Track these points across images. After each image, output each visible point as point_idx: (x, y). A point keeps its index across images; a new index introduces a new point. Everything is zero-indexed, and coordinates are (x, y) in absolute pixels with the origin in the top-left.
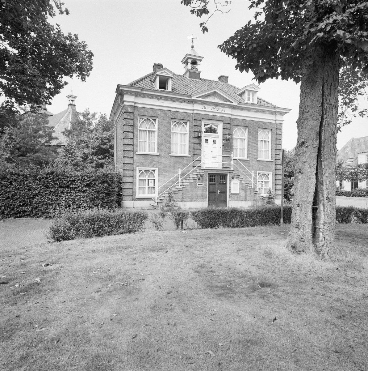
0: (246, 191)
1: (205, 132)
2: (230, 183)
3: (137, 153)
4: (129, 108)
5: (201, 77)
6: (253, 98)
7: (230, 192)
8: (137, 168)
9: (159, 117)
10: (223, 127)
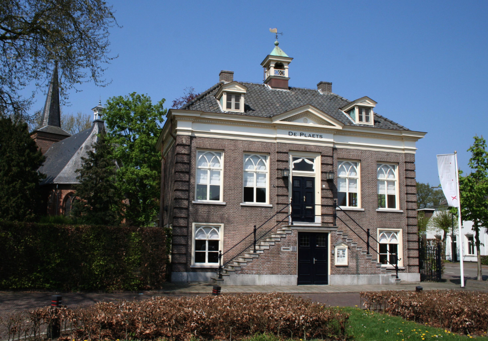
0: (357, 260)
1: (294, 169)
2: (333, 247)
3: (193, 202)
4: (184, 140)
6: (366, 117)
7: (332, 260)
8: (193, 224)
9: (226, 149)
10: (322, 161)
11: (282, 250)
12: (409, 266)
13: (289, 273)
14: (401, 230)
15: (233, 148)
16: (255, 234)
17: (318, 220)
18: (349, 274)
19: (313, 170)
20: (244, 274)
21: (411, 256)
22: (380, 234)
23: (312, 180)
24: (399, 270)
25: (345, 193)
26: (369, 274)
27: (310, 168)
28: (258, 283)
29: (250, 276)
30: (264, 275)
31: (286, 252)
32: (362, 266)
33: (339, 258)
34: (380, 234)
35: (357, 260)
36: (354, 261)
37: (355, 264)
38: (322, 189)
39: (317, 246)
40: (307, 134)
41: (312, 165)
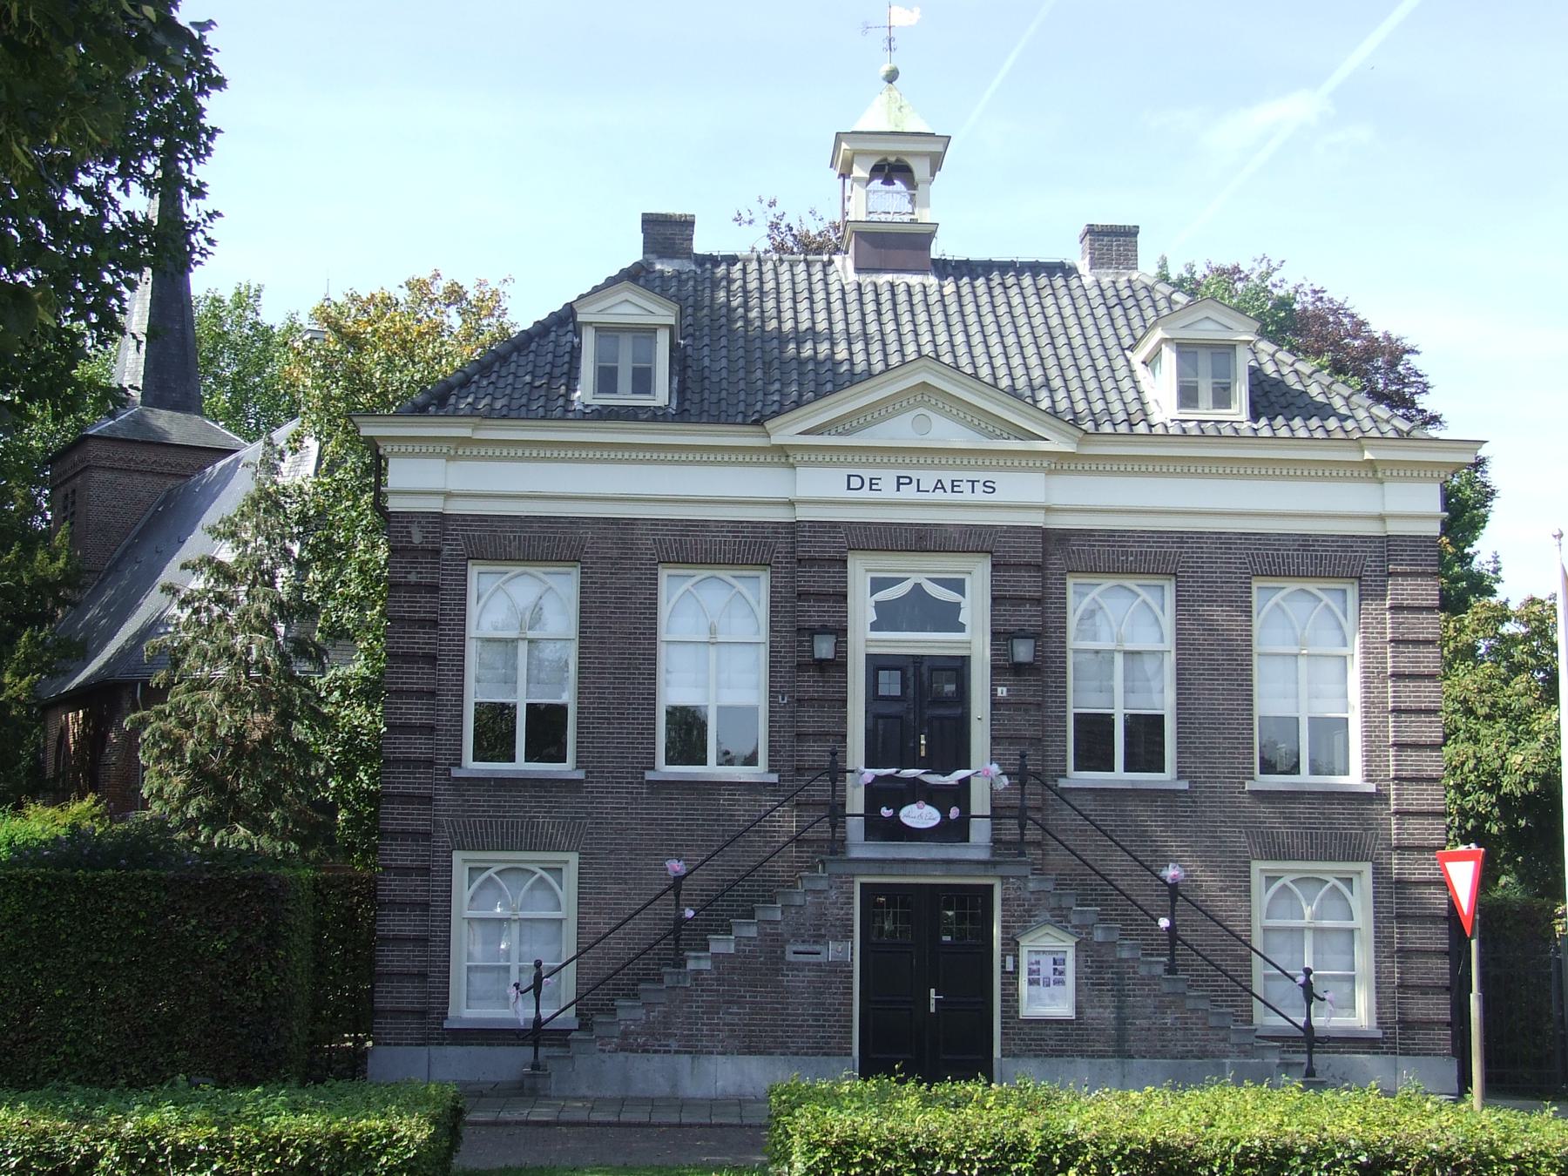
0: (1121, 995)
1: (875, 627)
2: (1012, 946)
7: (1011, 999)
8: (457, 856)
11: (790, 957)
12: (1406, 1025)
15: (615, 553)
16: (677, 895)
17: (980, 831)
18: (1082, 1053)
19: (960, 628)
20: (632, 1051)
21: (1413, 979)
23: (958, 667)
24: (1318, 1040)
25: (1108, 720)
26: (1172, 1058)
27: (947, 618)
28: (691, 1088)
30: (714, 1057)
31: (808, 964)
32: (1144, 1023)
33: (1042, 990)
34: (471, 881)
35: (1121, 995)
36: (1107, 1000)
37: (1109, 1014)
38: (996, 704)
39: (947, 938)
40: (928, 478)
41: (956, 607)
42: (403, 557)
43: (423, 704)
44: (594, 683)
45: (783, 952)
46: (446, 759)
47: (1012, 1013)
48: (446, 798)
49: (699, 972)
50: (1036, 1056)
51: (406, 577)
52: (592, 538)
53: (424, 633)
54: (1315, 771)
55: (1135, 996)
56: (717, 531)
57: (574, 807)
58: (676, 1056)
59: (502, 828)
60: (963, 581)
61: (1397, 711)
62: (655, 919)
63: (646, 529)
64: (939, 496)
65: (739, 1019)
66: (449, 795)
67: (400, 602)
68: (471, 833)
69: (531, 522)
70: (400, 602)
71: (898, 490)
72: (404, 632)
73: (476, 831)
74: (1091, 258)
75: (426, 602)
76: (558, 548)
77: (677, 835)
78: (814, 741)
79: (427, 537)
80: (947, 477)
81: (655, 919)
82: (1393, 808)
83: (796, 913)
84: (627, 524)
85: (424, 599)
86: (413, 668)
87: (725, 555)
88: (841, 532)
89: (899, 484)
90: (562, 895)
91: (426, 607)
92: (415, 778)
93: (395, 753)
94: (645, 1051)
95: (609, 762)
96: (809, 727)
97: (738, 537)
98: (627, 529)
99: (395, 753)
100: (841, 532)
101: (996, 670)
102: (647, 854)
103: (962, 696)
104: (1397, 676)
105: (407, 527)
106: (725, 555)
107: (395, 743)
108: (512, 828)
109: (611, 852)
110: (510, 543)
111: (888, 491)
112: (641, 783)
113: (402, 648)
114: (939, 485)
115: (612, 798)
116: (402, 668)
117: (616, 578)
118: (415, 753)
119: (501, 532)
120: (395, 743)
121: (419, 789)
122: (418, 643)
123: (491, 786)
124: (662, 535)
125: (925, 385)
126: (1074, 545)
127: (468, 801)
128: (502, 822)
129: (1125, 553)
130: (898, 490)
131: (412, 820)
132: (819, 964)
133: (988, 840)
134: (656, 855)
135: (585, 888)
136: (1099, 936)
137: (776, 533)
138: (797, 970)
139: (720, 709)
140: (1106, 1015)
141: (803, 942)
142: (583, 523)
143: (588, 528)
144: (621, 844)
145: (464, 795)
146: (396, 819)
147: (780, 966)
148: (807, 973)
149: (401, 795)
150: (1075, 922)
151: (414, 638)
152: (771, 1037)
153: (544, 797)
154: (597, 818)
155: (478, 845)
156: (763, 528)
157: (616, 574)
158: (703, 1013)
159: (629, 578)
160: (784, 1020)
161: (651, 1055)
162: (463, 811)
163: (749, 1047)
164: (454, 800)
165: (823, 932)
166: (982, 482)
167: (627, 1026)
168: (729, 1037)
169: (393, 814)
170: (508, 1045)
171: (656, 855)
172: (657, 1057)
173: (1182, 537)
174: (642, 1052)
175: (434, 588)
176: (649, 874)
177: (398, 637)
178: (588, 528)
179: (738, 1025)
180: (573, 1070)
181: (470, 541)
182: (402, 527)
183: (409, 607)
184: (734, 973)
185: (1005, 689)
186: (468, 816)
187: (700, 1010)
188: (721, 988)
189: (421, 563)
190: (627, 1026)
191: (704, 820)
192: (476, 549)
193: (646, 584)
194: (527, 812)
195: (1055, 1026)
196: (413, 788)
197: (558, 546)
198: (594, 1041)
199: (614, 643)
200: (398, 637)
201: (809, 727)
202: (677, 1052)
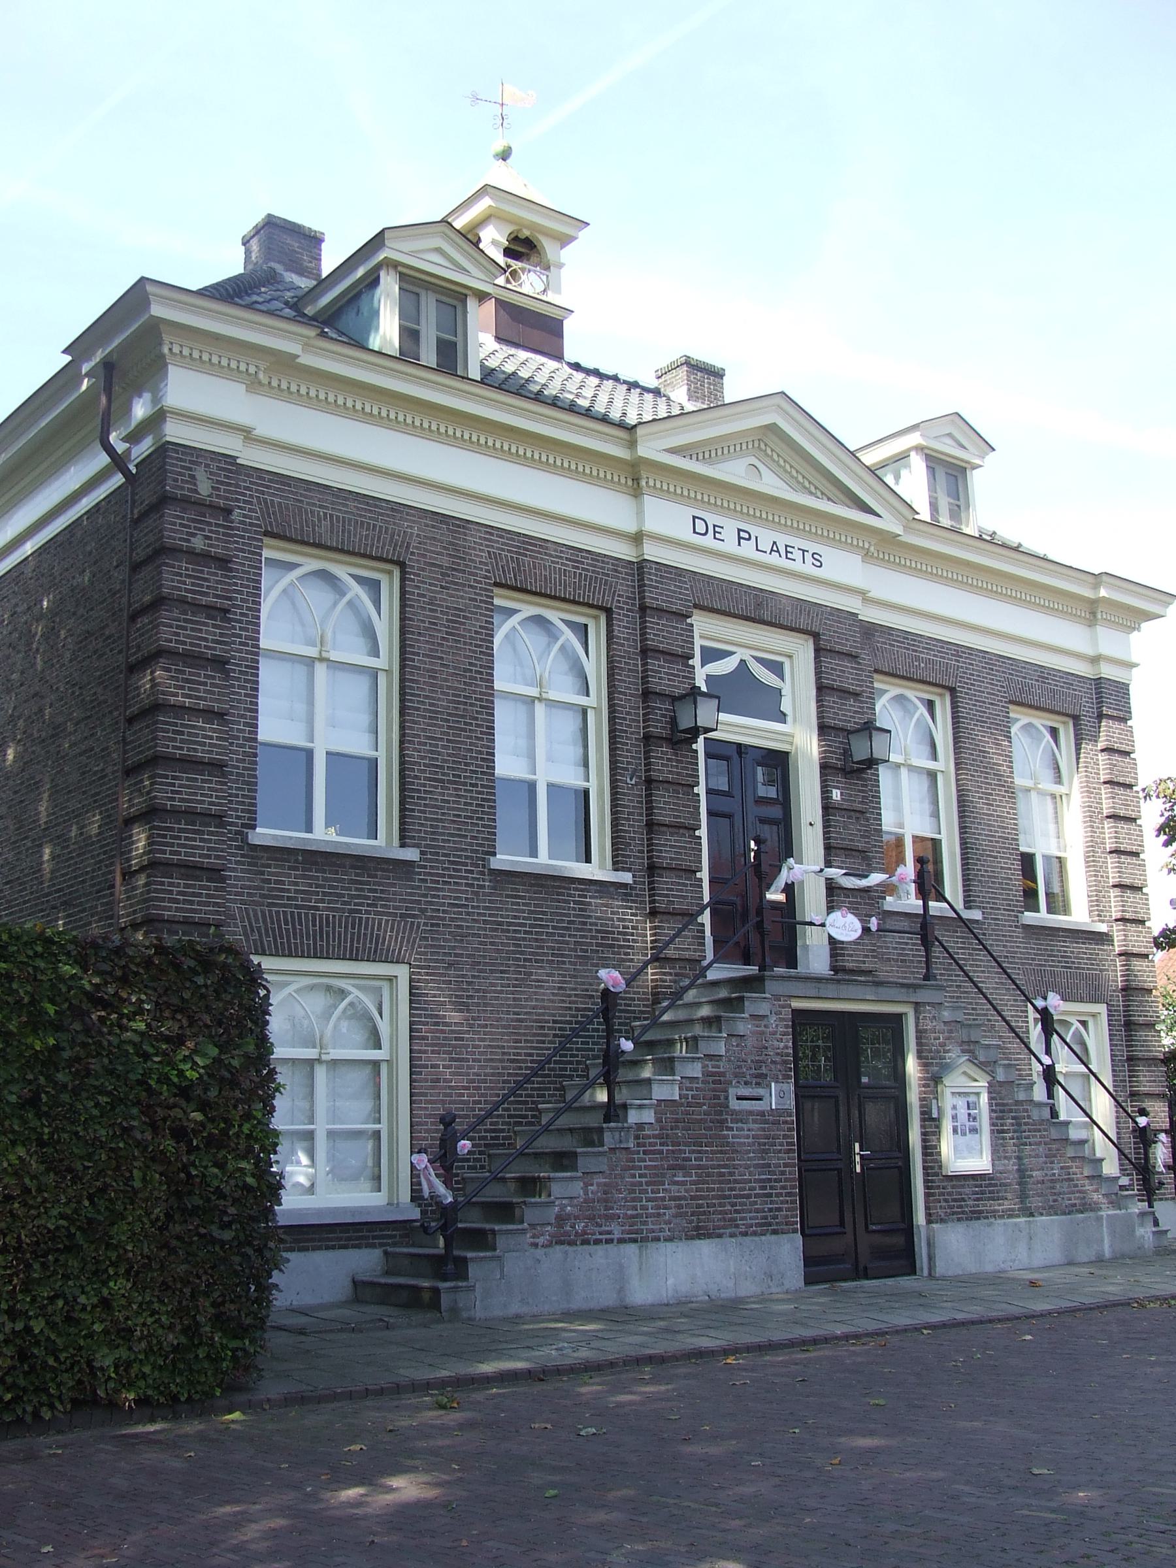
4: (201, 474)
5: (570, 354)
7: (930, 1150)
11: (734, 1104)
13: (769, 1227)
14: (1102, 1008)
15: (445, 561)
16: (607, 1020)
19: (782, 717)
20: (571, 1243)
22: (1035, 1026)
26: (1064, 1213)
28: (641, 1294)
29: (600, 1255)
30: (661, 1245)
31: (751, 1113)
38: (828, 808)
40: (766, 537)
42: (184, 510)
43: (214, 730)
44: (424, 730)
45: (727, 1098)
46: (238, 817)
47: (936, 1170)
48: (238, 874)
49: (640, 1126)
50: (959, 1220)
51: (188, 541)
52: (418, 536)
53: (214, 626)
54: (1051, 910)
55: (1030, 1145)
56: (557, 557)
57: (404, 901)
58: (622, 1246)
59: (315, 925)
60: (782, 664)
61: (1116, 852)
62: (502, 1061)
63: (480, 538)
64: (774, 559)
65: (686, 1191)
66: (242, 871)
67: (181, 575)
68: (273, 930)
69: (346, 499)
70: (181, 575)
71: (739, 544)
72: (186, 621)
73: (280, 928)
74: (689, 390)
75: (218, 582)
76: (378, 541)
77: (525, 946)
78: (672, 834)
79: (218, 489)
80: (782, 540)
81: (502, 1061)
82: (1117, 950)
83: (737, 1046)
84: (459, 526)
85: (212, 574)
86: (199, 675)
87: (565, 588)
88: (685, 583)
89: (740, 538)
90: (384, 1027)
91: (216, 589)
92: (202, 840)
93: (173, 799)
94: (586, 1242)
95: (444, 841)
96: (666, 815)
97: (578, 568)
98: (459, 532)
99: (173, 799)
100: (685, 583)
101: (825, 768)
102: (492, 971)
103: (785, 800)
104: (1114, 817)
105: (190, 469)
106: (565, 588)
107: (173, 785)
108: (328, 926)
109: (450, 965)
110: (320, 521)
111: (729, 545)
112: (482, 873)
113: (184, 643)
114: (775, 548)
115: (450, 890)
116: (184, 672)
117: (447, 594)
118: (202, 802)
119: (308, 504)
120: (173, 785)
121: (209, 857)
122: (206, 640)
123: (296, 861)
124: (498, 549)
125: (773, 428)
126: (878, 642)
127: (269, 881)
128: (314, 916)
129: (917, 659)
130: (739, 544)
131: (199, 903)
132: (762, 1114)
133: (828, 968)
134: (502, 972)
135: (420, 1016)
136: (1001, 1076)
137: (616, 571)
138: (741, 1121)
139: (550, 786)
140: (1010, 1168)
141: (746, 1083)
142: (408, 514)
143: (414, 522)
144: (461, 955)
145: (263, 873)
146: (177, 901)
147: (724, 1117)
148: (751, 1126)
149: (181, 865)
150: (982, 1059)
151: (200, 631)
152: (720, 1213)
153: (368, 883)
154: (432, 918)
155: (283, 949)
156: (603, 562)
157: (447, 588)
158: (647, 1184)
159: (462, 597)
160: (731, 1189)
161: (592, 1248)
162: (263, 896)
163: (697, 1228)
164: (249, 879)
165: (764, 1070)
166: (811, 553)
167: (563, 1207)
168: (676, 1216)
169: (171, 892)
170: (328, 1248)
171: (502, 972)
172: (600, 1250)
173: (960, 651)
174: (582, 1244)
175: (223, 563)
176: (497, 998)
177: (178, 627)
178: (414, 522)
179: (684, 1198)
180: (502, 1277)
181: (267, 507)
182: (183, 467)
183: (193, 584)
184: (677, 1128)
185: (839, 792)
186: (269, 905)
187: (643, 1180)
188: (665, 1148)
189: (210, 524)
190: (563, 1207)
191: (554, 928)
192: (276, 520)
193: (481, 608)
194: (345, 903)
195: (972, 1182)
196: (201, 856)
197: (379, 538)
198: (524, 1231)
199: (446, 680)
200: (178, 627)
201: (666, 815)
202: (621, 1241)
